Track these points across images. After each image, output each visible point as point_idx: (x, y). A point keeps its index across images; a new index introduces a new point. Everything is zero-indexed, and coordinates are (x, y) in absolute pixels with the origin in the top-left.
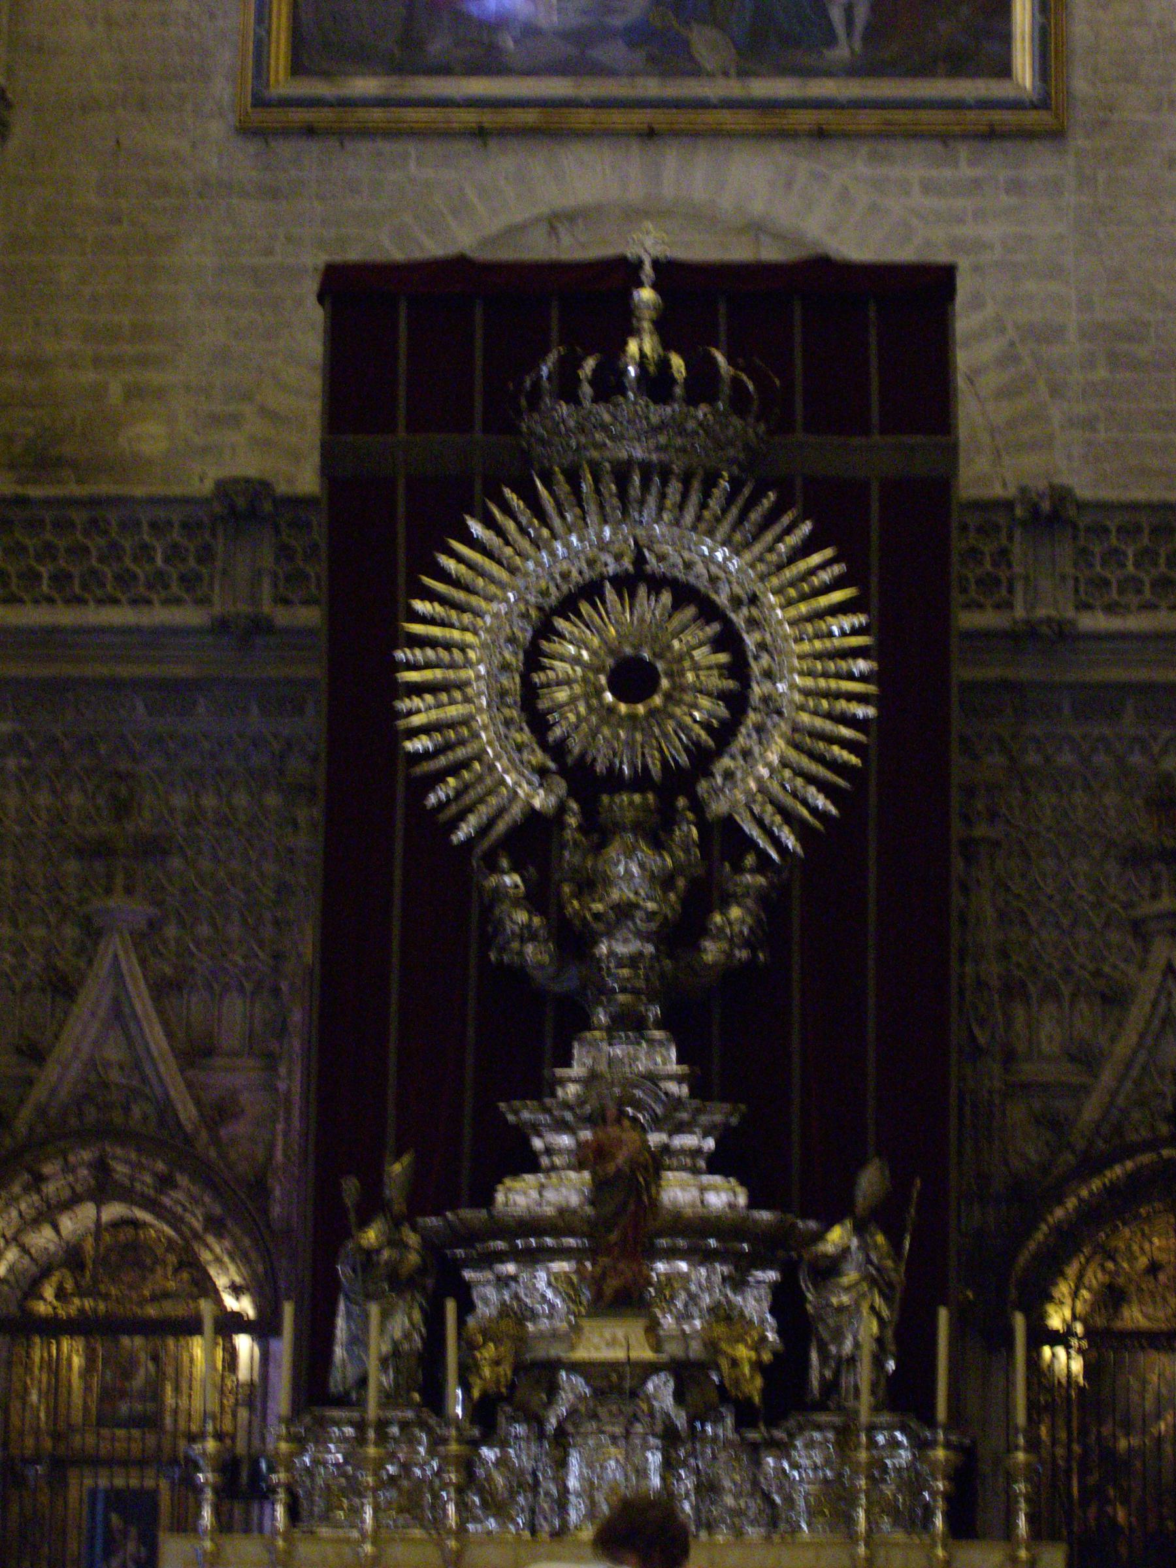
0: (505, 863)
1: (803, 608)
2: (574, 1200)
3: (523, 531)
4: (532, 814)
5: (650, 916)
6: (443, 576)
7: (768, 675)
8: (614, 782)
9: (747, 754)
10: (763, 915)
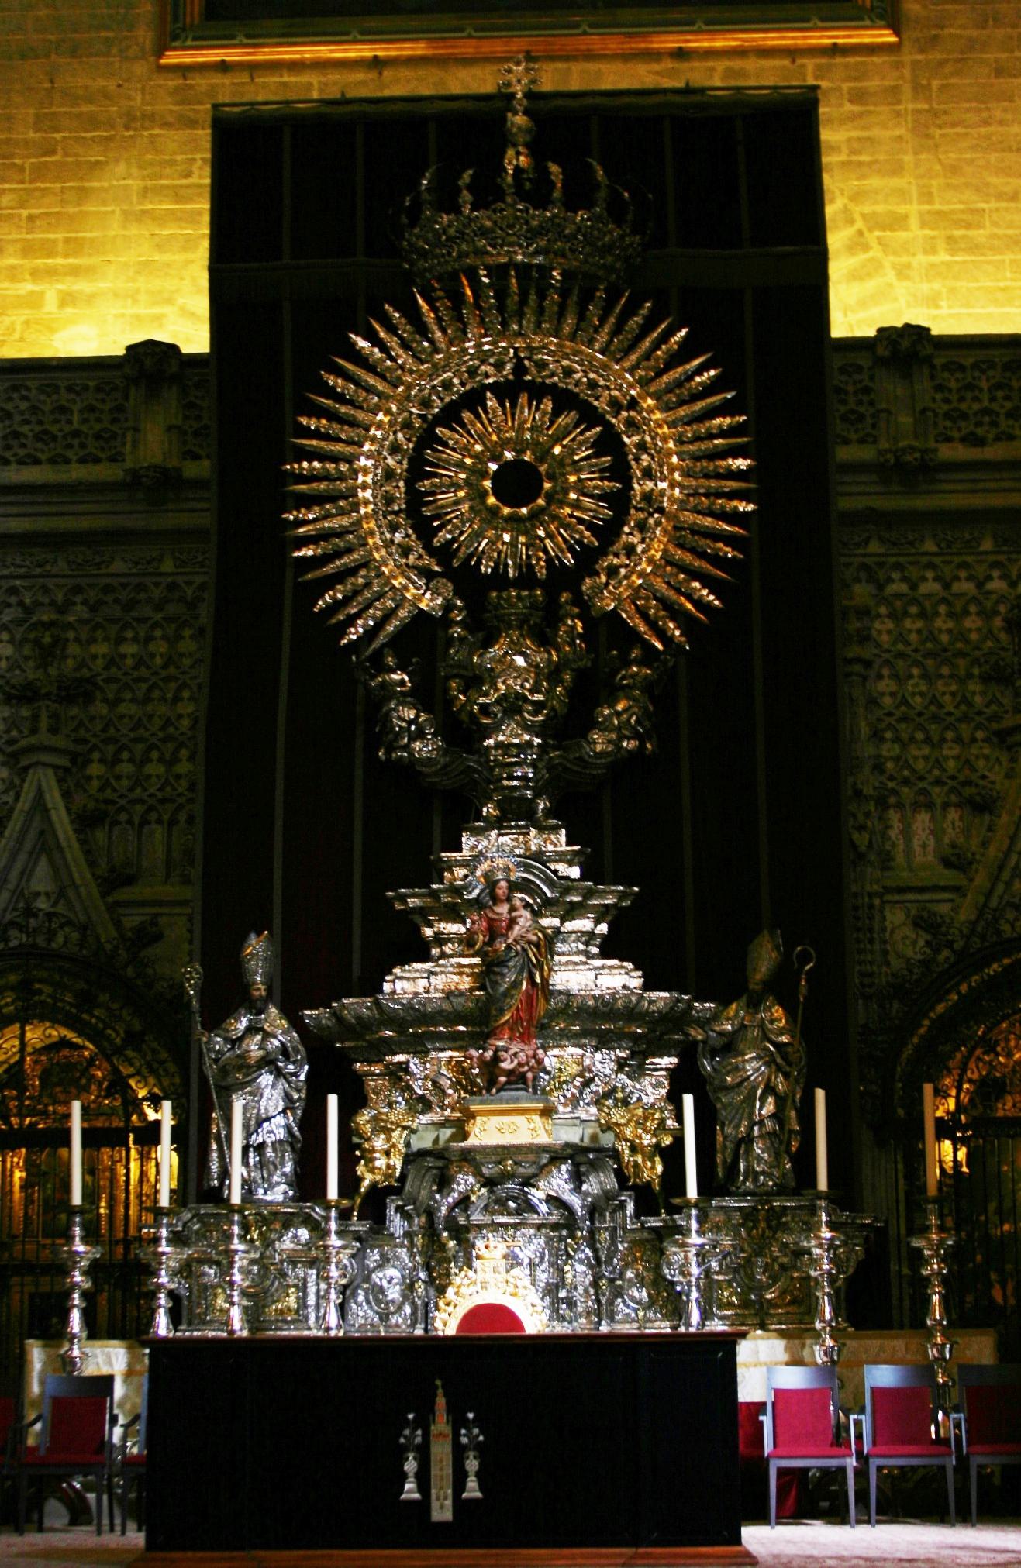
0: (390, 661)
1: (682, 412)
2: (466, 983)
3: (405, 345)
4: (421, 617)
5: (538, 707)
6: (331, 393)
7: (648, 474)
8: (498, 578)
9: (630, 550)
10: (651, 708)
